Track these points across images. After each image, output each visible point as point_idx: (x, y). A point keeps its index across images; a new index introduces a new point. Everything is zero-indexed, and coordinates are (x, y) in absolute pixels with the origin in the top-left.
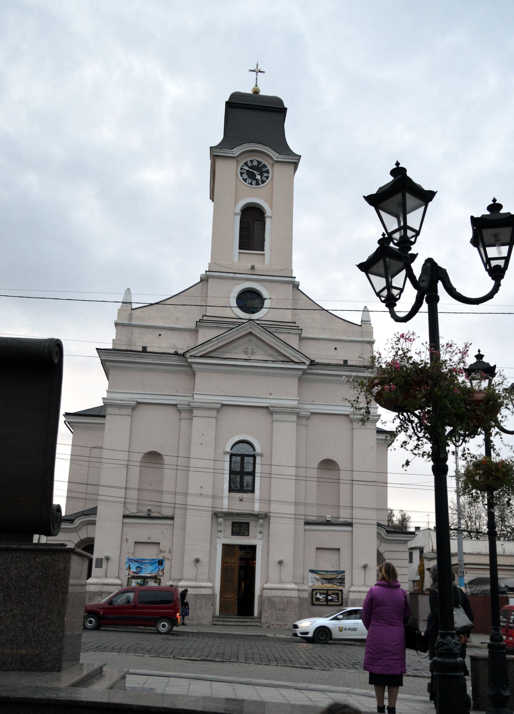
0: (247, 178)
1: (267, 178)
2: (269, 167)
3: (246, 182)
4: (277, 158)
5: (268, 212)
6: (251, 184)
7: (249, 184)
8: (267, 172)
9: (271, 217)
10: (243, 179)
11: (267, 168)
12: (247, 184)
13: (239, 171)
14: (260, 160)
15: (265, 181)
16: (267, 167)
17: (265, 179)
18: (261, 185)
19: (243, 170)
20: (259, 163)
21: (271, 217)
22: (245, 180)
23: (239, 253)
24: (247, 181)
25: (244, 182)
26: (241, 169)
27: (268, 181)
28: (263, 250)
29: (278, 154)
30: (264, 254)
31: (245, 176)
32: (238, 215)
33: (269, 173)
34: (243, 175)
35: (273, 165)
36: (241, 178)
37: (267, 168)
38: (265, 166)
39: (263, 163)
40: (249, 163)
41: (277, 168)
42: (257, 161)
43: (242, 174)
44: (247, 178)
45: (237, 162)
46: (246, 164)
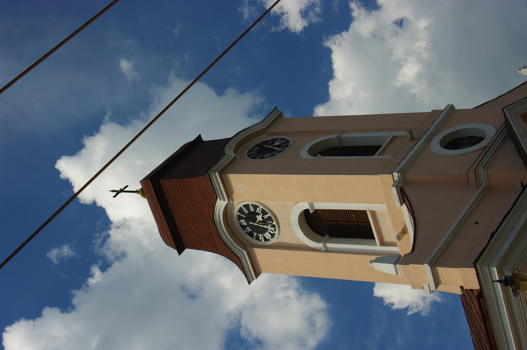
1: (255, 207)
2: (241, 205)
3: (274, 234)
7: (275, 230)
8: (247, 206)
9: (311, 205)
10: (271, 238)
11: (242, 207)
12: (276, 233)
15: (262, 209)
16: (241, 208)
17: (258, 209)
19: (260, 238)
20: (239, 218)
21: (311, 205)
22: (273, 235)
24: (272, 233)
28: (365, 211)
29: (218, 200)
31: (267, 235)
34: (268, 238)
37: (242, 207)
38: (241, 210)
39: (239, 213)
42: (239, 220)
46: (251, 234)
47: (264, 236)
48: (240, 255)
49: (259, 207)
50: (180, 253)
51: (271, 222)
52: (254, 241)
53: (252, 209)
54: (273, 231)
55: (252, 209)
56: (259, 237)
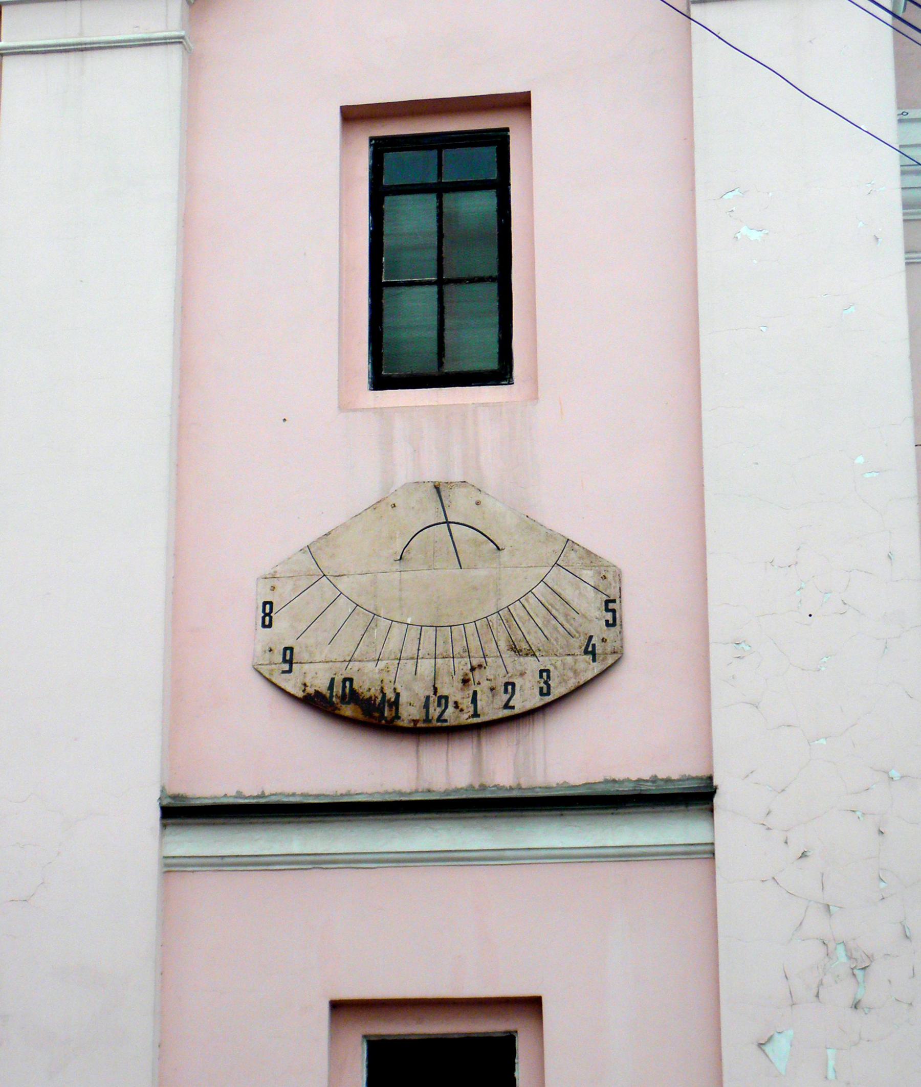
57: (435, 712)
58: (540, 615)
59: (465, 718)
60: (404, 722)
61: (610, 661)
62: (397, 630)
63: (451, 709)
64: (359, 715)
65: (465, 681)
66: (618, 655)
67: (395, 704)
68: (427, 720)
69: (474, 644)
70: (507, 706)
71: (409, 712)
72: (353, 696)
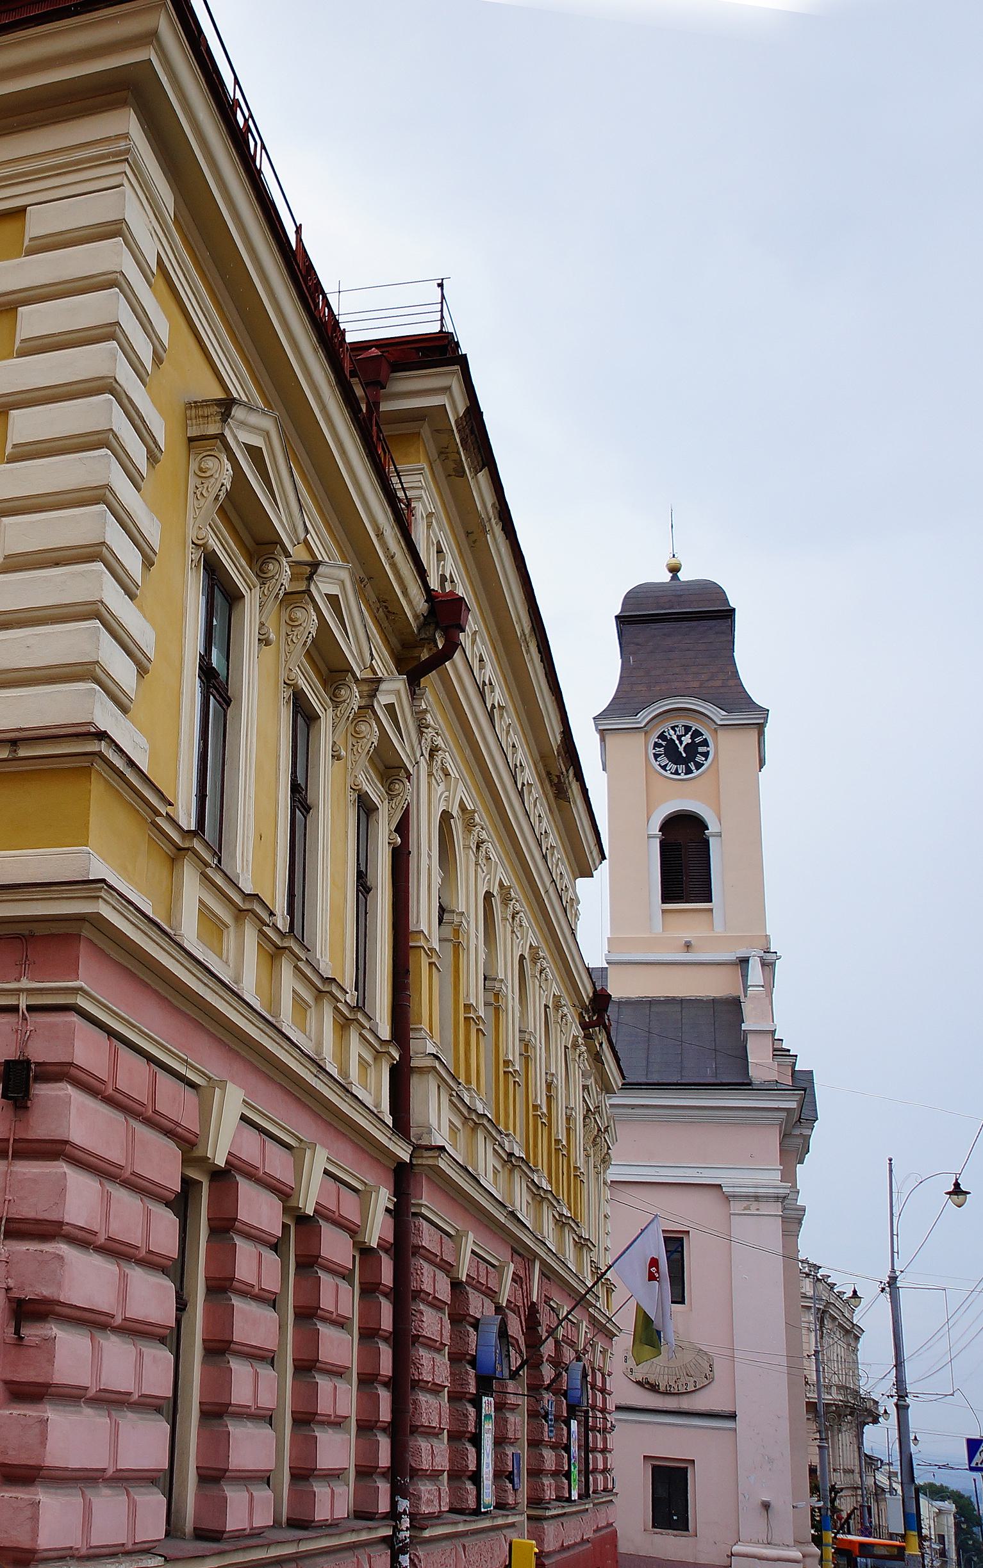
0: (666, 765)
2: (707, 735)
4: (722, 720)
5: (713, 827)
6: (677, 773)
7: (671, 773)
8: (705, 743)
9: (719, 835)
10: (660, 765)
12: (668, 774)
13: (651, 752)
14: (689, 723)
15: (703, 764)
16: (703, 735)
17: (704, 759)
18: (696, 773)
19: (658, 749)
20: (687, 729)
22: (664, 768)
23: (664, 911)
25: (662, 771)
26: (656, 745)
27: (707, 764)
28: (711, 901)
30: (711, 910)
31: (664, 760)
32: (657, 837)
33: (708, 746)
35: (716, 730)
36: (656, 764)
37: (704, 737)
39: (693, 729)
40: (666, 734)
41: (722, 735)
42: (683, 726)
43: (656, 756)
44: (666, 765)
45: (646, 733)
47: (662, 754)
48: (638, 719)
49: (706, 760)
50: (616, 617)
51: (684, 772)
52: (654, 739)
53: (701, 749)
54: (670, 770)
55: (701, 749)
56: (660, 748)
57: (668, 1389)
58: (694, 1367)
59: (676, 1391)
60: (661, 1391)
61: (711, 1380)
62: (658, 1367)
63: (672, 1388)
64: (650, 1388)
65: (675, 1382)
66: (713, 1378)
67: (659, 1386)
68: (667, 1391)
69: (677, 1373)
70: (686, 1389)
71: (662, 1389)
72: (648, 1383)
